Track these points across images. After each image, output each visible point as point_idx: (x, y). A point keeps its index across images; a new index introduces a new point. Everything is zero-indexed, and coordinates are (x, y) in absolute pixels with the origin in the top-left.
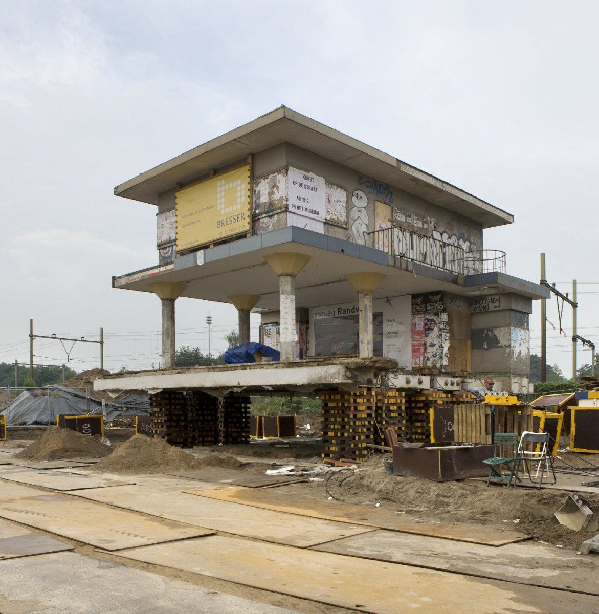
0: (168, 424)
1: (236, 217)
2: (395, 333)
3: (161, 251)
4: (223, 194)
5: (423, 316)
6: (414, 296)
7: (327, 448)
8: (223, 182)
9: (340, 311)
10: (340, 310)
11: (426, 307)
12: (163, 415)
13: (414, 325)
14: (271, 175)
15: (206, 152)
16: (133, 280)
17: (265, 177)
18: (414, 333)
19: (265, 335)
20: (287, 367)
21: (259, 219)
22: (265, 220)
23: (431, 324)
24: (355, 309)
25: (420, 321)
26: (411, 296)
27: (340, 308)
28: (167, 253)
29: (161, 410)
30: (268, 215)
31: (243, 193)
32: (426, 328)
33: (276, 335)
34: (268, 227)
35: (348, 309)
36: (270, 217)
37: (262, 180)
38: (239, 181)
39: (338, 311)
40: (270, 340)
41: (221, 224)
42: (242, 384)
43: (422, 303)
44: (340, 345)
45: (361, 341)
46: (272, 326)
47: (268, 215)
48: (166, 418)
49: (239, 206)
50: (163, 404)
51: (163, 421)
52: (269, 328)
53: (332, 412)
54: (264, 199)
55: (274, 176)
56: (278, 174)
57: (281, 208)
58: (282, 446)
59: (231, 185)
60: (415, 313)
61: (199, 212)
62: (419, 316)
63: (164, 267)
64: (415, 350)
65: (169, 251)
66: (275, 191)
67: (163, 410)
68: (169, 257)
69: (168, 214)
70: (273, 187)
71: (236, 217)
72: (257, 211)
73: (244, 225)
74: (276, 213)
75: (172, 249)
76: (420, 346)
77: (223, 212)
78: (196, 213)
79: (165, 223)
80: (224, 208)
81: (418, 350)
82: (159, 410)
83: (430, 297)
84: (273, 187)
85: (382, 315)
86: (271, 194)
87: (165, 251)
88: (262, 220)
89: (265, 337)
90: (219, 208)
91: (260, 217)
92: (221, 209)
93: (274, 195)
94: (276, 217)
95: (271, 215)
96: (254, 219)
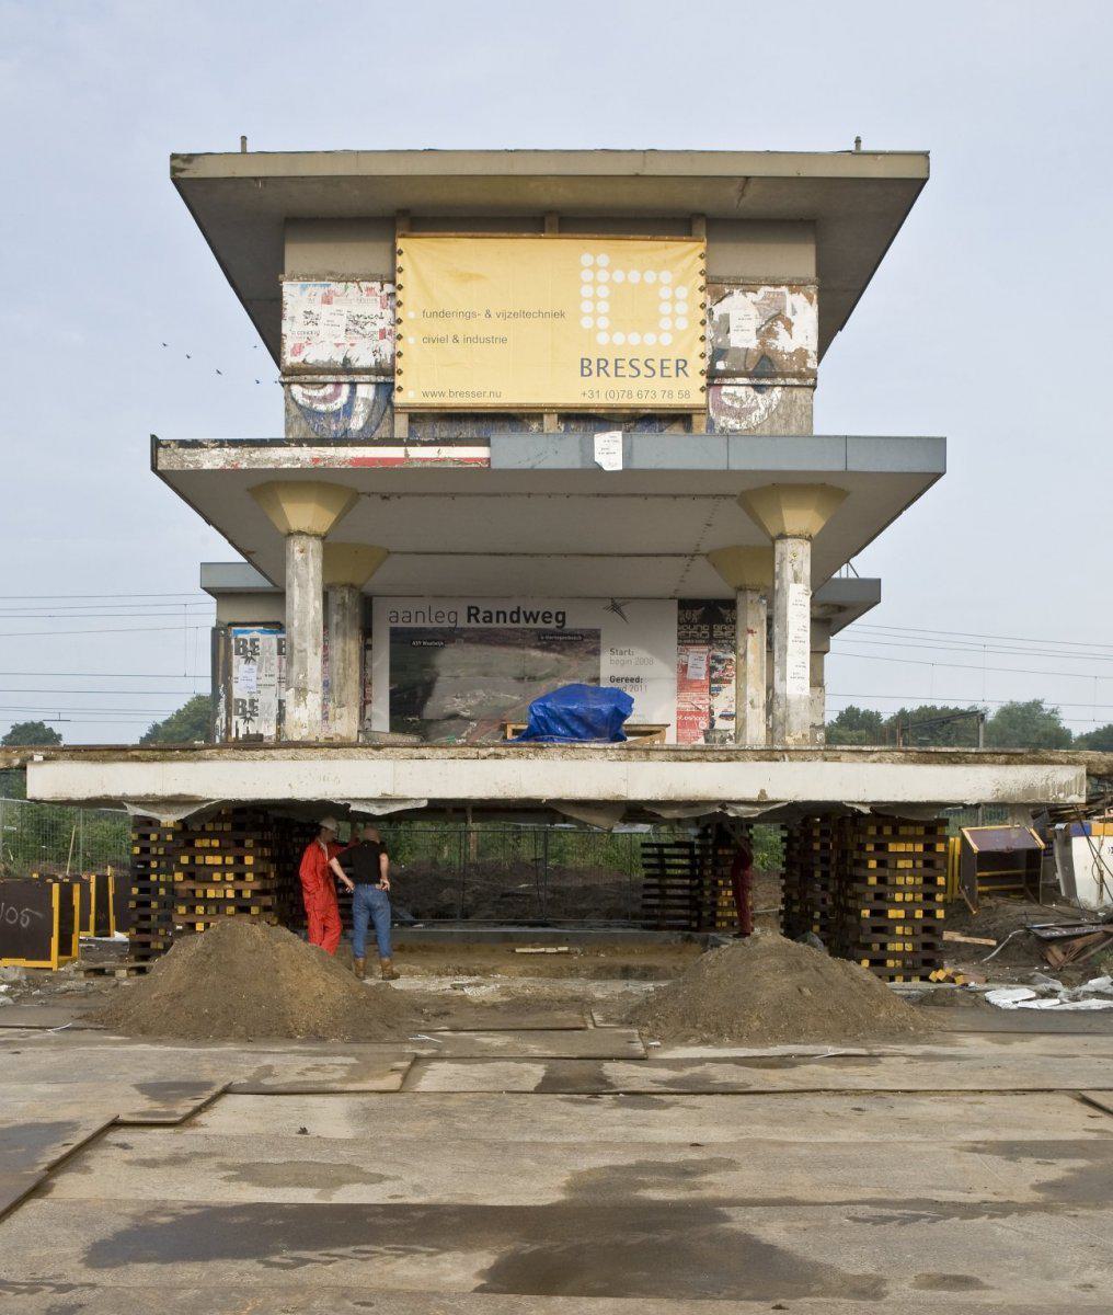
0: (268, 900)
1: (656, 365)
2: (632, 680)
3: (297, 390)
4: (604, 292)
5: (706, 649)
6: (685, 604)
7: (876, 947)
8: (603, 260)
9: (475, 615)
10: (473, 611)
11: (711, 631)
12: (250, 876)
13: (684, 669)
14: (772, 289)
15: (637, 176)
16: (268, 460)
17: (749, 285)
18: (684, 684)
19: (237, 653)
20: (913, 762)
21: (721, 385)
22: (741, 391)
23: (725, 669)
24: (522, 615)
25: (698, 660)
26: (676, 601)
27: (473, 607)
28: (325, 399)
29: (240, 860)
30: (755, 381)
31: (682, 308)
32: (713, 677)
33: (276, 657)
34: (750, 411)
35: (498, 613)
36: (758, 388)
37: (736, 292)
38: (666, 276)
39: (469, 615)
40: (255, 668)
41: (594, 367)
42: (771, 796)
43: (701, 622)
44: (475, 697)
45: (752, 703)
46: (259, 631)
47: (755, 381)
48: (257, 885)
49: (667, 339)
50: (249, 843)
51: (247, 894)
52: (256, 635)
53: (901, 864)
54: (744, 337)
55: (778, 294)
56: (792, 292)
57: (800, 375)
58: (542, 950)
59: (634, 276)
60: (685, 641)
61: (504, 315)
62: (695, 649)
63: (437, 448)
65: (336, 395)
66: (780, 327)
67: (249, 860)
68: (336, 414)
69: (338, 287)
70: (775, 318)
71: (656, 365)
72: (720, 365)
73: (687, 391)
74: (782, 382)
75: (353, 392)
76: (699, 713)
77: (602, 338)
78: (488, 315)
79: (324, 311)
80: (610, 331)
81: (693, 725)
82: (230, 860)
83: (721, 609)
84: (775, 318)
85: (599, 637)
86: (766, 333)
88: (725, 389)
89: (237, 660)
90: (586, 323)
91: (728, 381)
92: (596, 330)
93: (775, 338)
94: (777, 393)
95: (762, 386)
96: (713, 378)
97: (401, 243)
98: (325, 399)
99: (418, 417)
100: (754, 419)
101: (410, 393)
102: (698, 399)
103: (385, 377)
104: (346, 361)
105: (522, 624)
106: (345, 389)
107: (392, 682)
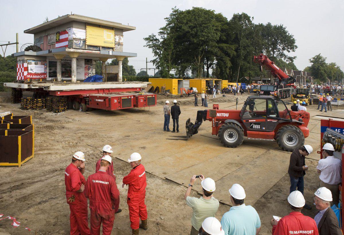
28: (77, 42)
64: (85, 74)
87: (77, 41)
97: (87, 26)
98: (77, 42)
99: (89, 46)
100: (118, 49)
101: (88, 43)
102: (114, 47)
103: (85, 41)
104: (80, 38)
105: (66, 61)
106: (80, 41)
107: (49, 68)
